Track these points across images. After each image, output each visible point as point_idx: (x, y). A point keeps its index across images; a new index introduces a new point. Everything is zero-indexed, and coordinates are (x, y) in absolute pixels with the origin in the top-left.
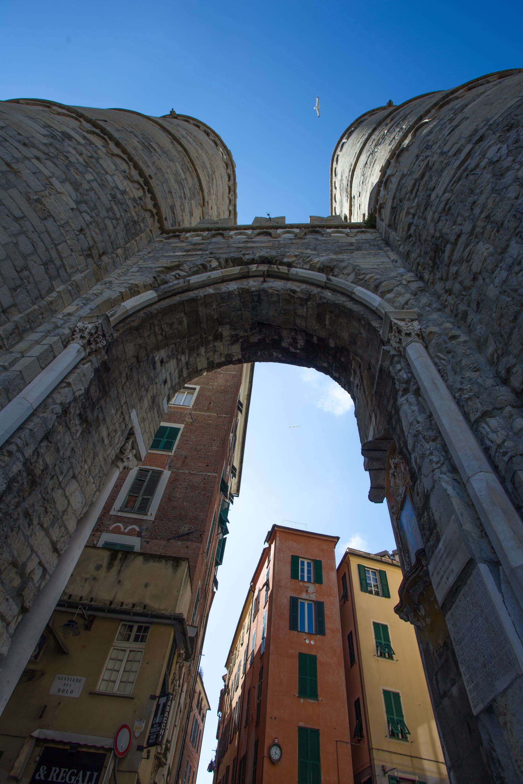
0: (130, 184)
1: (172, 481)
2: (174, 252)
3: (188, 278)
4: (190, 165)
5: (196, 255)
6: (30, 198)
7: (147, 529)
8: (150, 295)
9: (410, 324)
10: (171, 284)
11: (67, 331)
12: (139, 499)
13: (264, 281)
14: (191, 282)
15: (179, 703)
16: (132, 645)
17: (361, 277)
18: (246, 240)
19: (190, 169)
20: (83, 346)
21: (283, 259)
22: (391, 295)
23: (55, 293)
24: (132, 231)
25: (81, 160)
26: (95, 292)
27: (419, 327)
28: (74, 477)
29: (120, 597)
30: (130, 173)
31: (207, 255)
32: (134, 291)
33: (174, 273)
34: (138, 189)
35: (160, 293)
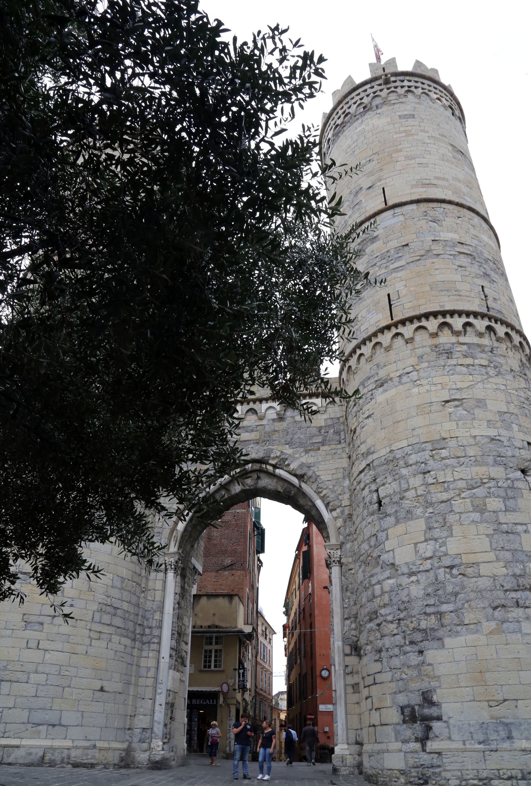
17: (320, 490)
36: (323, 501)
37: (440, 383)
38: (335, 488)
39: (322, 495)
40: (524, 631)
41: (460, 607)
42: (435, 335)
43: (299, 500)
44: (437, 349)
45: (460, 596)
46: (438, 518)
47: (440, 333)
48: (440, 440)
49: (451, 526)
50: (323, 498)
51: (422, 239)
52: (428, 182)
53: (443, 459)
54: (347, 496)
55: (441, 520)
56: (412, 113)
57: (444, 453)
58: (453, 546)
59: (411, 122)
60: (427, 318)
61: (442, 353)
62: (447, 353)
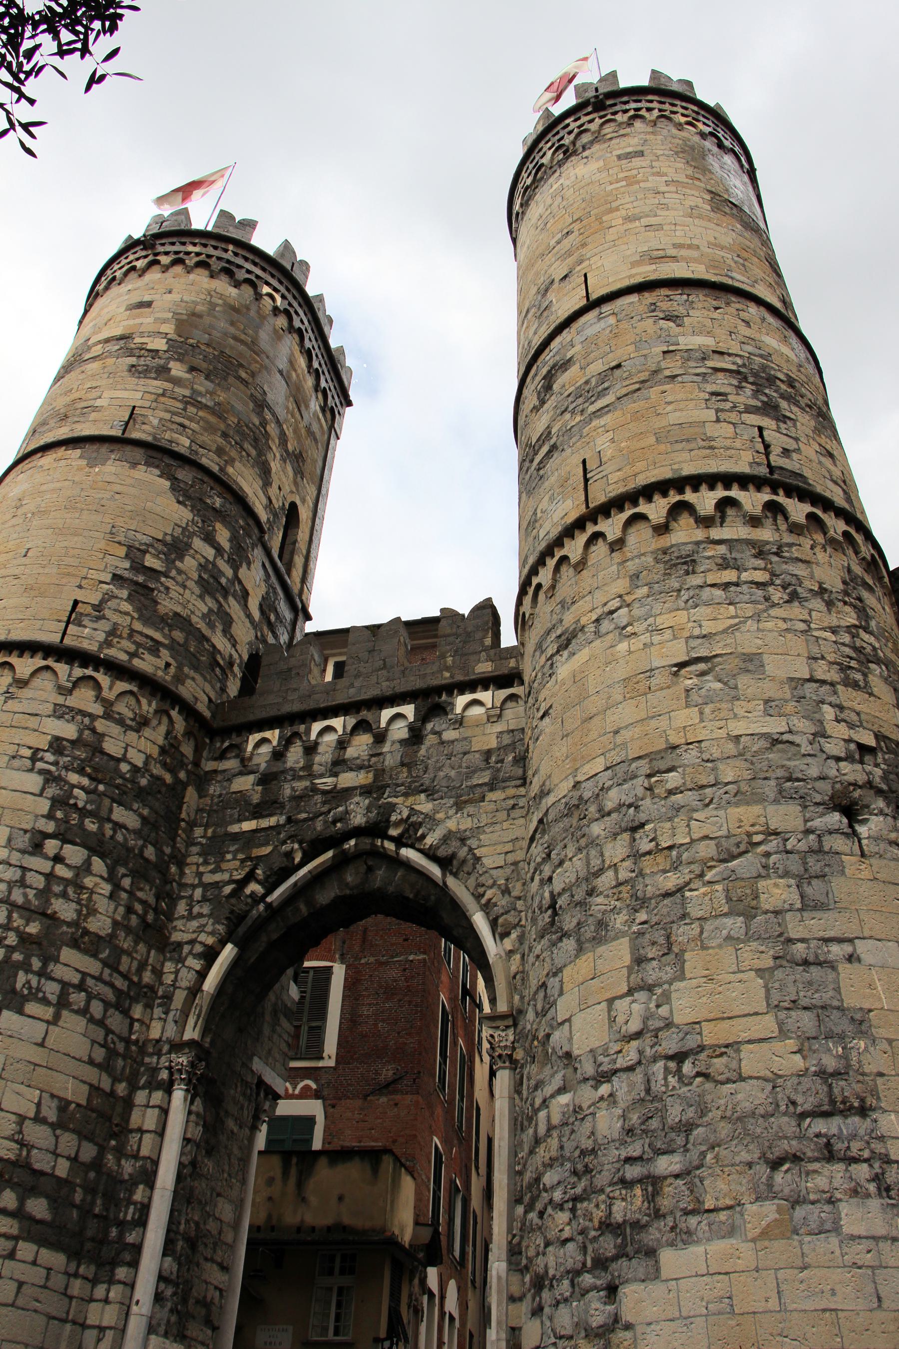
0: (147, 732)
1: (350, 985)
2: (240, 821)
3: (269, 899)
5: (271, 828)
6: (76, 940)
7: (329, 1083)
8: (228, 952)
9: (503, 1034)
10: (249, 921)
11: (164, 1075)
12: (304, 1030)
13: (370, 869)
14: (275, 905)
17: (481, 890)
19: (218, 502)
20: (187, 1091)
21: (388, 828)
22: (508, 944)
23: (136, 1024)
24: (174, 809)
25: (85, 781)
26: (169, 982)
27: (511, 1038)
28: (219, 1195)
29: (310, 1219)
30: (142, 716)
32: (210, 956)
33: (248, 891)
34: (160, 723)
36: (487, 914)
37: (673, 627)
39: (483, 901)
40: (846, 1230)
41: (696, 1163)
42: (662, 529)
44: (667, 558)
45: (695, 1132)
47: (673, 525)
48: (667, 749)
49: (683, 951)
50: (486, 908)
51: (645, 352)
52: (661, 253)
53: (671, 792)
55: (662, 940)
56: (640, 148)
57: (673, 779)
58: (685, 1005)
59: (637, 162)
60: (650, 499)
61: (675, 565)
62: (685, 563)
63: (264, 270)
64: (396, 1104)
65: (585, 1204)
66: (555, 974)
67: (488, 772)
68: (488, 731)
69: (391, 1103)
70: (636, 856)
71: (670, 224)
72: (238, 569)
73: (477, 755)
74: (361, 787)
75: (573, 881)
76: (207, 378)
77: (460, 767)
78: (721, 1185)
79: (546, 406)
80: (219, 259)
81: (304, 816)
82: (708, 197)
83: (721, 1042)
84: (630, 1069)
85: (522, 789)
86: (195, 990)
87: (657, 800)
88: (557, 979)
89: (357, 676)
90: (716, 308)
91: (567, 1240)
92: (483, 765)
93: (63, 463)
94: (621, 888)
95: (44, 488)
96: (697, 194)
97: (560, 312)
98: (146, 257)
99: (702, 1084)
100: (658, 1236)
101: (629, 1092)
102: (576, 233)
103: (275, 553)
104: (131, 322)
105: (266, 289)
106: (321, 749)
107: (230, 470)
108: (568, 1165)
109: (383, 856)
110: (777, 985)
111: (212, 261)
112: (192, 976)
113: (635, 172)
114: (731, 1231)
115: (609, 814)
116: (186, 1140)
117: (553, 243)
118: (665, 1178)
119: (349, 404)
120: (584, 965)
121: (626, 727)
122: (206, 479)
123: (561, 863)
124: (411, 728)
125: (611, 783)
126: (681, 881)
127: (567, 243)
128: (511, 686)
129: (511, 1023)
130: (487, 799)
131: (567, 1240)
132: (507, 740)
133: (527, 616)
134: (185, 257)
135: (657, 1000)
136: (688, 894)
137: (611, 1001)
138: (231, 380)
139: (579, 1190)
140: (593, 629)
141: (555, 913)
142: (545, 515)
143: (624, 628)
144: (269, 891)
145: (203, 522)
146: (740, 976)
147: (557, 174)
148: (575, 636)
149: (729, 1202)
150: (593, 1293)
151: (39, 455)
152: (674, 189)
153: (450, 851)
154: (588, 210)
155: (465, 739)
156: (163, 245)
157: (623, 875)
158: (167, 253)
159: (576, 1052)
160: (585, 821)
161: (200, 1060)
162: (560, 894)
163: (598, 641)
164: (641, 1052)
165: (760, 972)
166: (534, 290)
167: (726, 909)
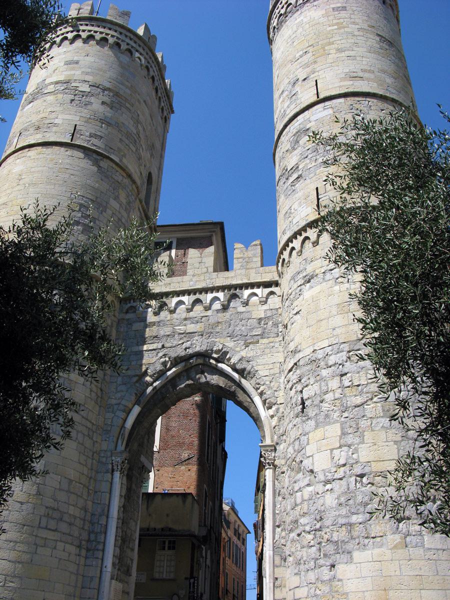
2: (138, 345)
3: (155, 384)
4: (119, 176)
8: (137, 410)
11: (110, 466)
15: (206, 565)
16: (168, 552)
17: (258, 386)
18: (184, 315)
19: (120, 179)
20: (121, 474)
21: (212, 353)
22: (271, 412)
27: (273, 455)
29: (153, 525)
31: (161, 349)
35: (142, 406)
36: (261, 398)
38: (272, 384)
39: (259, 391)
43: (239, 396)
46: (352, 423)
50: (261, 394)
52: (355, 74)
54: (281, 393)
55: (354, 426)
56: (344, 5)
58: (364, 454)
59: (343, 14)
63: (135, 42)
64: (189, 470)
65: (320, 532)
66: (304, 435)
67: (260, 329)
68: (259, 309)
69: (187, 469)
70: (343, 387)
71: (360, 56)
72: (130, 212)
73: (255, 320)
74: (199, 332)
75: (313, 395)
76: (111, 109)
77: (247, 326)
78: (378, 527)
79: (296, 152)
80: (113, 36)
81: (171, 345)
82: (378, 39)
83: (379, 470)
84: (341, 479)
85: (276, 338)
86: (123, 427)
87: (352, 363)
88: (306, 437)
89: (193, 276)
90: (382, 110)
91: (312, 546)
92: (258, 326)
93: (41, 156)
94: (336, 401)
95: (33, 170)
96: (372, 36)
97: (303, 100)
98: (72, 32)
99: (371, 487)
100: (352, 546)
101: (340, 488)
102: (311, 54)
103: (143, 203)
104: (69, 73)
105: (137, 55)
106: (177, 311)
107: (124, 160)
108: (313, 516)
109: (210, 365)
110: (402, 448)
111: (109, 37)
112: (121, 421)
113: (342, 20)
114: (381, 547)
115: (330, 367)
116: (121, 496)
117: (298, 56)
118: (355, 524)
119: (173, 112)
120: (319, 433)
121: (339, 327)
122: (114, 166)
123: (307, 386)
124: (223, 305)
125: (331, 353)
126: (363, 401)
127: (306, 59)
128: (271, 287)
129: (273, 448)
130: (260, 342)
131: (312, 546)
132: (269, 314)
133: (286, 261)
134: (94, 34)
135: (352, 451)
136: (366, 407)
137: (332, 450)
138: (123, 109)
139: (318, 526)
140: (322, 277)
141: (304, 408)
142: (296, 212)
143: (337, 279)
144: (155, 381)
145: (114, 190)
146: (387, 443)
147: (299, 12)
148: (312, 278)
149: (382, 535)
150: (325, 567)
151: (27, 150)
152: (361, 33)
153: (243, 367)
154: (317, 40)
155: (249, 312)
156: (82, 25)
157: (337, 395)
158: (84, 31)
159: (315, 470)
160: (319, 369)
161: (126, 460)
162: (306, 400)
163: (325, 283)
164: (345, 472)
165: (396, 442)
166: (287, 81)
167: (382, 415)
